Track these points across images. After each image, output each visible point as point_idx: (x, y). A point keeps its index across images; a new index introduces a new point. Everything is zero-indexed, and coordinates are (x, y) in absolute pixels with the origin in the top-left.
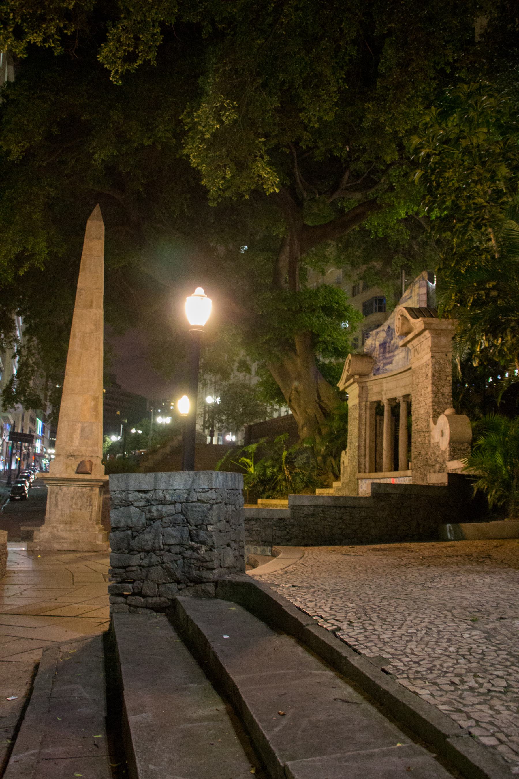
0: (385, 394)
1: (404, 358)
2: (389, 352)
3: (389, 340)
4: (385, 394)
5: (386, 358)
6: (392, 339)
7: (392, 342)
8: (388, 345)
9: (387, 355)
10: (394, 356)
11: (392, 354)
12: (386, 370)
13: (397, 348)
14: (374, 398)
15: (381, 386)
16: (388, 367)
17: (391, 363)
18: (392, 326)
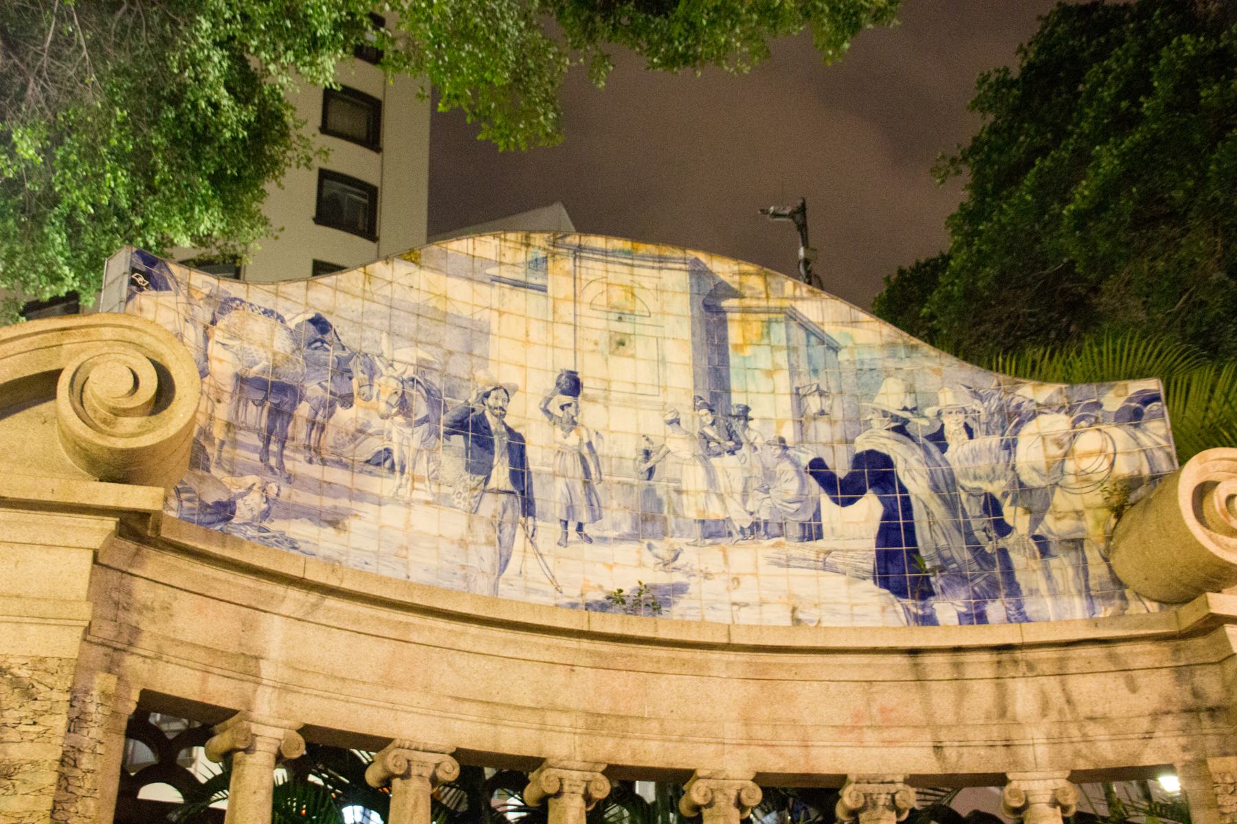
0: (284, 688)
1: (463, 543)
2: (315, 453)
3: (314, 389)
4: (284, 688)
5: (290, 479)
6: (347, 400)
7: (343, 415)
8: (304, 410)
9: (297, 464)
10: (357, 495)
11: (338, 476)
12: (293, 545)
13: (382, 460)
14: (180, 682)
15: (248, 626)
16: (300, 530)
17: (334, 521)
18: (346, 333)
